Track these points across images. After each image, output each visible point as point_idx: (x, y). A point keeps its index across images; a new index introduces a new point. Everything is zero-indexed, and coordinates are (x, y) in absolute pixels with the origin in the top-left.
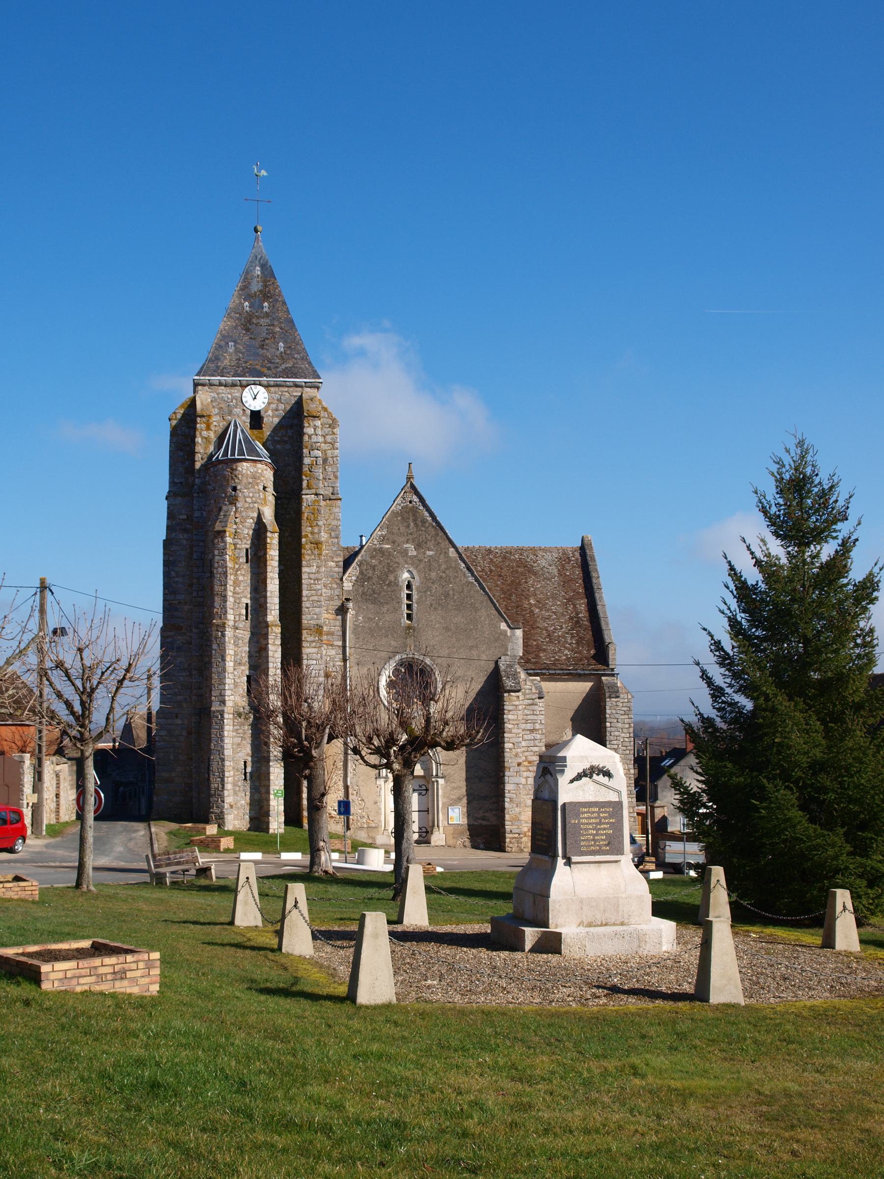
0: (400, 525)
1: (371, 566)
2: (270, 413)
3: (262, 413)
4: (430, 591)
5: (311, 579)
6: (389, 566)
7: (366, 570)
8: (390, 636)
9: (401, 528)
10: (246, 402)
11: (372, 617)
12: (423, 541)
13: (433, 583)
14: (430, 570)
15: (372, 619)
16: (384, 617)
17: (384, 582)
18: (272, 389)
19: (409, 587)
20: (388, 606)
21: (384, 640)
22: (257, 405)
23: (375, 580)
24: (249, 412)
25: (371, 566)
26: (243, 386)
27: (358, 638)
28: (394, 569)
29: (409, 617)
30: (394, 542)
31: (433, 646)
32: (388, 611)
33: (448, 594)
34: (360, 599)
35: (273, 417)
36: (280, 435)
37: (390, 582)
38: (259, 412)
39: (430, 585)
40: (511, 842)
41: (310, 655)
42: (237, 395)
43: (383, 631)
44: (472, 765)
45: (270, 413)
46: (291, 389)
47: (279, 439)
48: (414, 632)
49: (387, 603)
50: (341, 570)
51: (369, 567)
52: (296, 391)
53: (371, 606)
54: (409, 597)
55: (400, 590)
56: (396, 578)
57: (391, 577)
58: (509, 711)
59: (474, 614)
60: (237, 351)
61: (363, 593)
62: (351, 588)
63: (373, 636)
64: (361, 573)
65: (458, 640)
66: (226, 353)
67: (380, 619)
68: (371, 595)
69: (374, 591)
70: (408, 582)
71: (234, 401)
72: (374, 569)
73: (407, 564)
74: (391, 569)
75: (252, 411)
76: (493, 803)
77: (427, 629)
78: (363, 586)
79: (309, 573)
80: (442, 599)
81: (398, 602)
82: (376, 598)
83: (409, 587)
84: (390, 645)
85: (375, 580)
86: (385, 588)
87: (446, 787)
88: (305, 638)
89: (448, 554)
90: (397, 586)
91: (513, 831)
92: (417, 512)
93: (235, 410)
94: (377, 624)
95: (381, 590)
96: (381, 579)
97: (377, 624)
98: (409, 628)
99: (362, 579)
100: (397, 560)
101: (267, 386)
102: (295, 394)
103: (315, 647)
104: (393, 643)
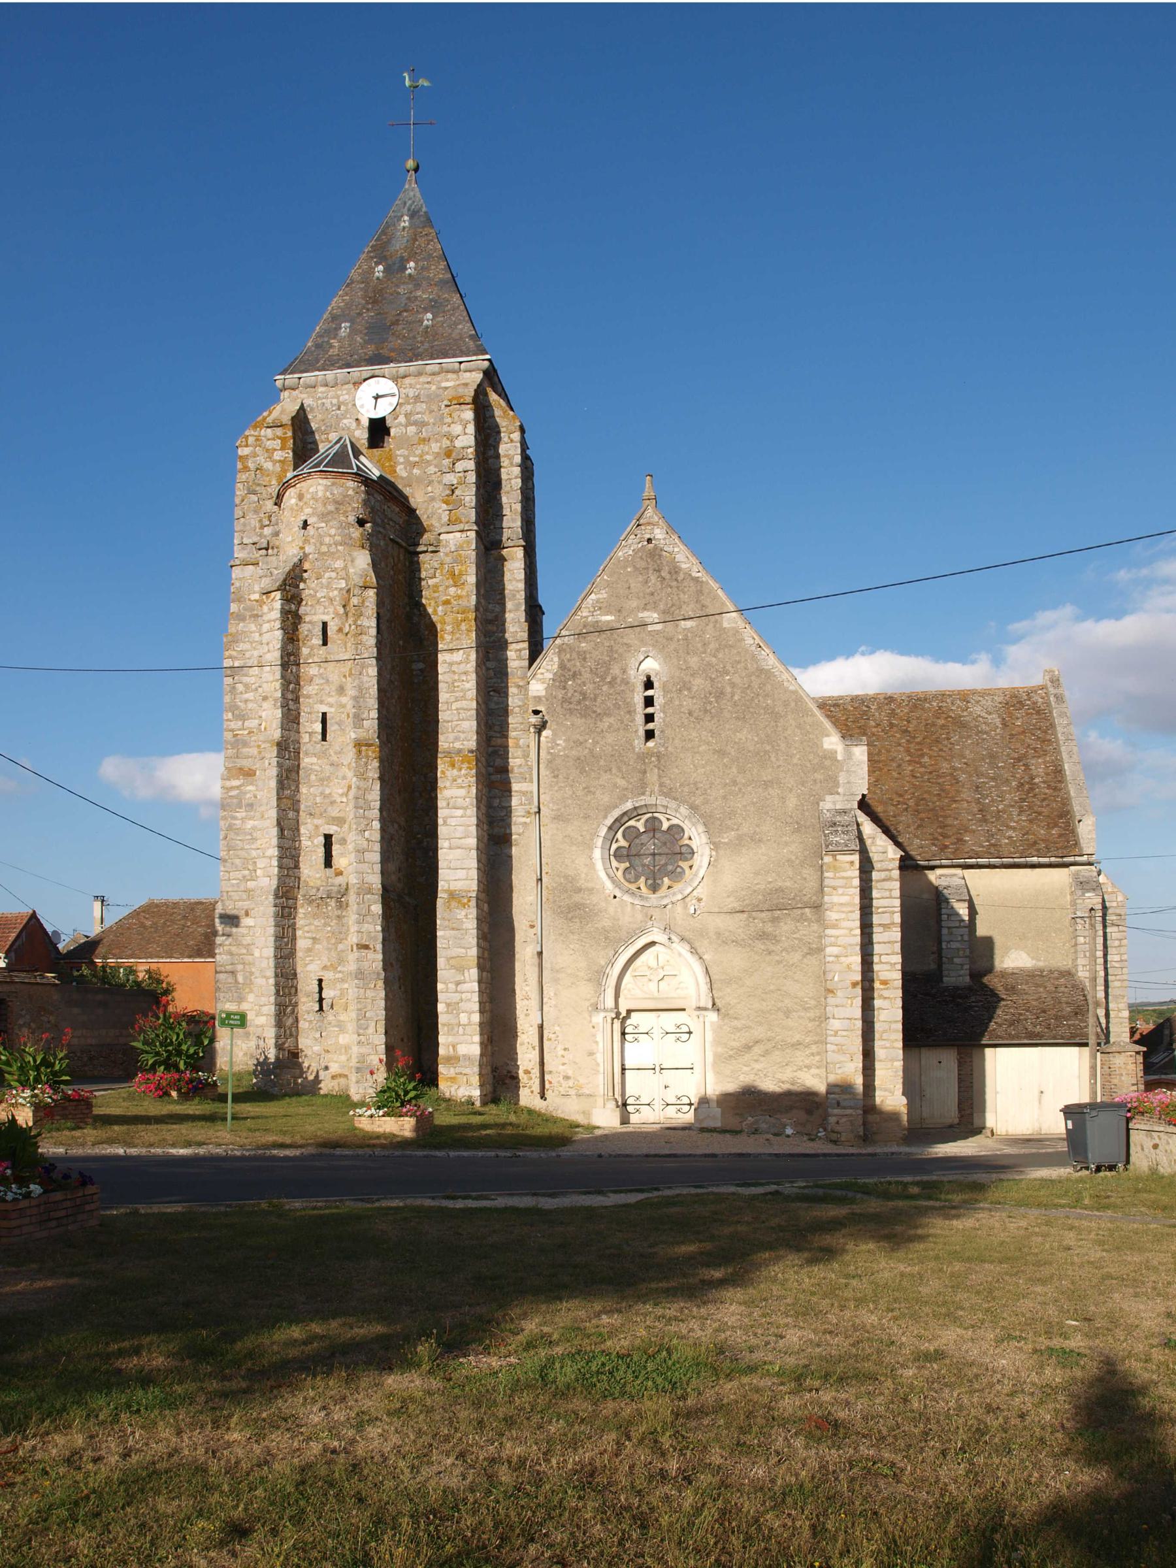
0: (631, 581)
1: (578, 653)
2: (402, 419)
3: (389, 423)
4: (689, 689)
5: (454, 672)
6: (612, 650)
7: (569, 660)
8: (614, 771)
9: (632, 586)
10: (362, 406)
11: (581, 739)
12: (673, 605)
13: (692, 675)
14: (688, 653)
15: (581, 743)
16: (603, 737)
17: (603, 678)
18: (407, 381)
19: (649, 685)
20: (612, 720)
21: (606, 777)
22: (382, 410)
23: (586, 675)
24: (366, 423)
25: (578, 653)
26: (357, 384)
27: (556, 777)
28: (621, 655)
29: (650, 735)
30: (619, 611)
31: (695, 783)
32: (609, 727)
33: (722, 693)
34: (559, 709)
35: (406, 426)
36: (418, 452)
37: (614, 679)
38: (383, 419)
39: (687, 679)
40: (838, 1123)
41: (452, 801)
42: (347, 397)
43: (602, 763)
44: (772, 987)
45: (402, 419)
46: (438, 378)
47: (417, 459)
48: (659, 760)
49: (609, 715)
50: (526, 663)
51: (574, 655)
52: (447, 380)
53: (579, 721)
54: (649, 701)
55: (633, 691)
56: (624, 671)
57: (616, 670)
58: (834, 888)
59: (773, 724)
60: (353, 331)
61: (565, 700)
62: (543, 693)
63: (582, 771)
64: (562, 666)
65: (742, 771)
66: (334, 338)
67: (596, 743)
68: (579, 702)
69: (584, 694)
70: (649, 677)
71: (342, 408)
72: (585, 659)
73: (645, 645)
74: (616, 656)
75: (372, 421)
76: (813, 1054)
77: (682, 755)
78: (564, 688)
79: (451, 664)
80: (711, 703)
81: (629, 712)
82: (587, 707)
83: (649, 685)
84: (615, 786)
85: (586, 675)
86: (605, 688)
87: (720, 1027)
88: (443, 772)
89: (721, 624)
90: (628, 683)
91: (843, 1104)
92: (660, 556)
93: (345, 421)
94: (591, 751)
95: (598, 692)
96: (597, 675)
97: (591, 751)
98: (649, 754)
99: (565, 675)
100: (625, 641)
101: (395, 379)
102: (444, 384)
103: (462, 787)
104: (622, 783)
